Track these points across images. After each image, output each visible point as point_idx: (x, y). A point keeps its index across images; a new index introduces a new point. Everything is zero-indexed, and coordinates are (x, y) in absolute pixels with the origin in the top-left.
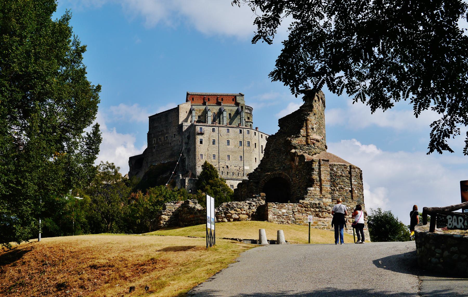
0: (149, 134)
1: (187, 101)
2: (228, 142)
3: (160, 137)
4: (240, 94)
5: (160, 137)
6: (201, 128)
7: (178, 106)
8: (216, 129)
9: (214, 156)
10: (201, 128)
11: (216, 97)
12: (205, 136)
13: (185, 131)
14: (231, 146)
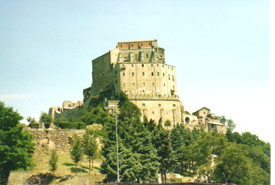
0: (93, 73)
1: (117, 47)
2: (143, 73)
3: (99, 74)
4: (155, 40)
5: (99, 74)
6: (123, 65)
7: (110, 51)
8: (134, 65)
9: (134, 84)
10: (123, 65)
11: (137, 44)
12: (126, 70)
13: (114, 68)
14: (146, 76)
